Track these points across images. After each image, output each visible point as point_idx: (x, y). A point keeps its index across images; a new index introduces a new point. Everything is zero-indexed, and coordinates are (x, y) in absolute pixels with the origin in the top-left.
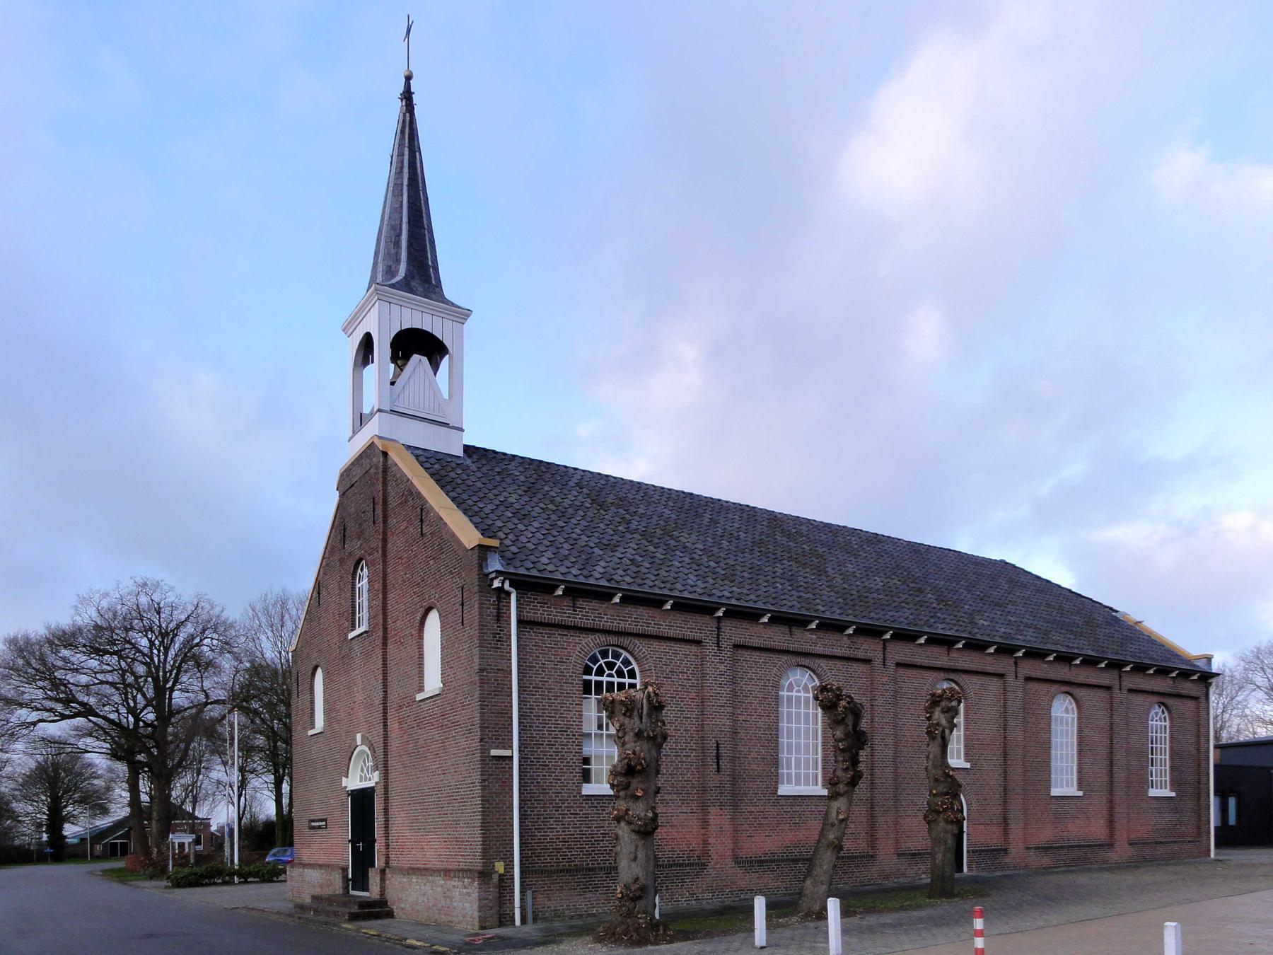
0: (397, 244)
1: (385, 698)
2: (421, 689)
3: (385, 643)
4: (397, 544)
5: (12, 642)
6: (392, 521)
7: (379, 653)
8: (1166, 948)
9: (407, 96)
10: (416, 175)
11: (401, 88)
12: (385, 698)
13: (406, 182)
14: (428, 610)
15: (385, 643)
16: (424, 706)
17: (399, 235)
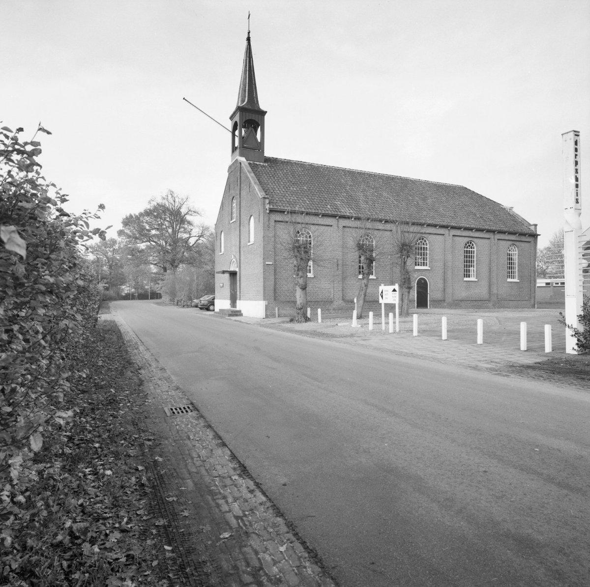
0: (245, 94)
1: (240, 244)
2: (249, 242)
3: (240, 226)
4: (244, 193)
5: (220, 310)
6: (242, 185)
7: (238, 228)
8: (482, 338)
9: (249, 39)
10: (251, 66)
11: (246, 36)
12: (240, 244)
13: (248, 69)
14: (251, 216)
15: (240, 226)
16: (250, 247)
17: (246, 87)
